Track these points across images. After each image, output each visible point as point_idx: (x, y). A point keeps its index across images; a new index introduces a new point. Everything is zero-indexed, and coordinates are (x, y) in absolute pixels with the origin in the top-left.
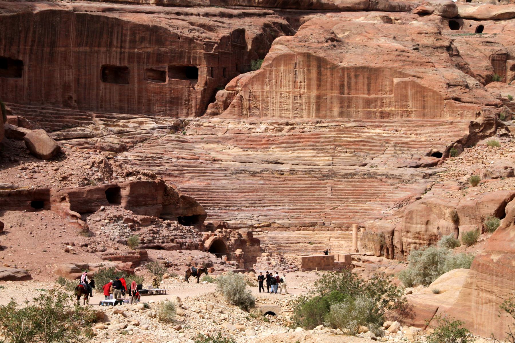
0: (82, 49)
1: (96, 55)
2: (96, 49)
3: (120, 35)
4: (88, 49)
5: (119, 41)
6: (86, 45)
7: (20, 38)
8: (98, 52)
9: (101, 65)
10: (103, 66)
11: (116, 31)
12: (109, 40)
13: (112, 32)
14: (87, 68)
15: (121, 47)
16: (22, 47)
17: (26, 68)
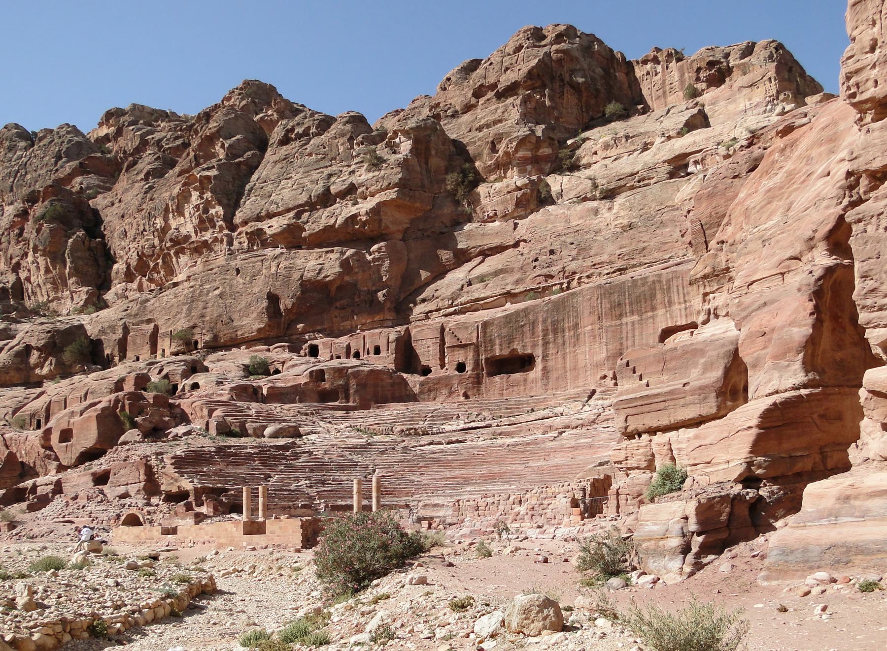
0: (624, 320)
1: (651, 320)
2: (650, 314)
3: (681, 289)
4: (636, 318)
5: (681, 295)
6: (632, 313)
7: (523, 333)
8: (653, 317)
9: (660, 330)
10: (663, 331)
11: (675, 286)
12: (666, 299)
13: (669, 288)
14: (637, 338)
15: (685, 301)
16: (528, 340)
17: (539, 360)
